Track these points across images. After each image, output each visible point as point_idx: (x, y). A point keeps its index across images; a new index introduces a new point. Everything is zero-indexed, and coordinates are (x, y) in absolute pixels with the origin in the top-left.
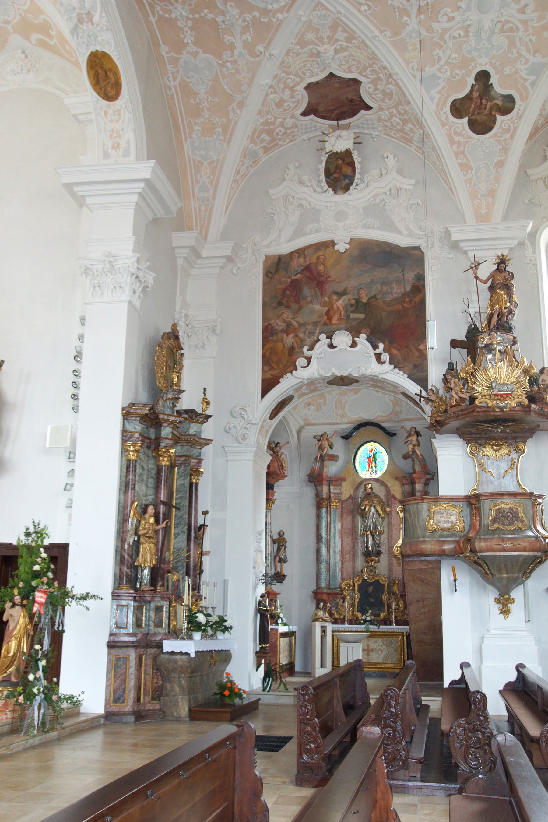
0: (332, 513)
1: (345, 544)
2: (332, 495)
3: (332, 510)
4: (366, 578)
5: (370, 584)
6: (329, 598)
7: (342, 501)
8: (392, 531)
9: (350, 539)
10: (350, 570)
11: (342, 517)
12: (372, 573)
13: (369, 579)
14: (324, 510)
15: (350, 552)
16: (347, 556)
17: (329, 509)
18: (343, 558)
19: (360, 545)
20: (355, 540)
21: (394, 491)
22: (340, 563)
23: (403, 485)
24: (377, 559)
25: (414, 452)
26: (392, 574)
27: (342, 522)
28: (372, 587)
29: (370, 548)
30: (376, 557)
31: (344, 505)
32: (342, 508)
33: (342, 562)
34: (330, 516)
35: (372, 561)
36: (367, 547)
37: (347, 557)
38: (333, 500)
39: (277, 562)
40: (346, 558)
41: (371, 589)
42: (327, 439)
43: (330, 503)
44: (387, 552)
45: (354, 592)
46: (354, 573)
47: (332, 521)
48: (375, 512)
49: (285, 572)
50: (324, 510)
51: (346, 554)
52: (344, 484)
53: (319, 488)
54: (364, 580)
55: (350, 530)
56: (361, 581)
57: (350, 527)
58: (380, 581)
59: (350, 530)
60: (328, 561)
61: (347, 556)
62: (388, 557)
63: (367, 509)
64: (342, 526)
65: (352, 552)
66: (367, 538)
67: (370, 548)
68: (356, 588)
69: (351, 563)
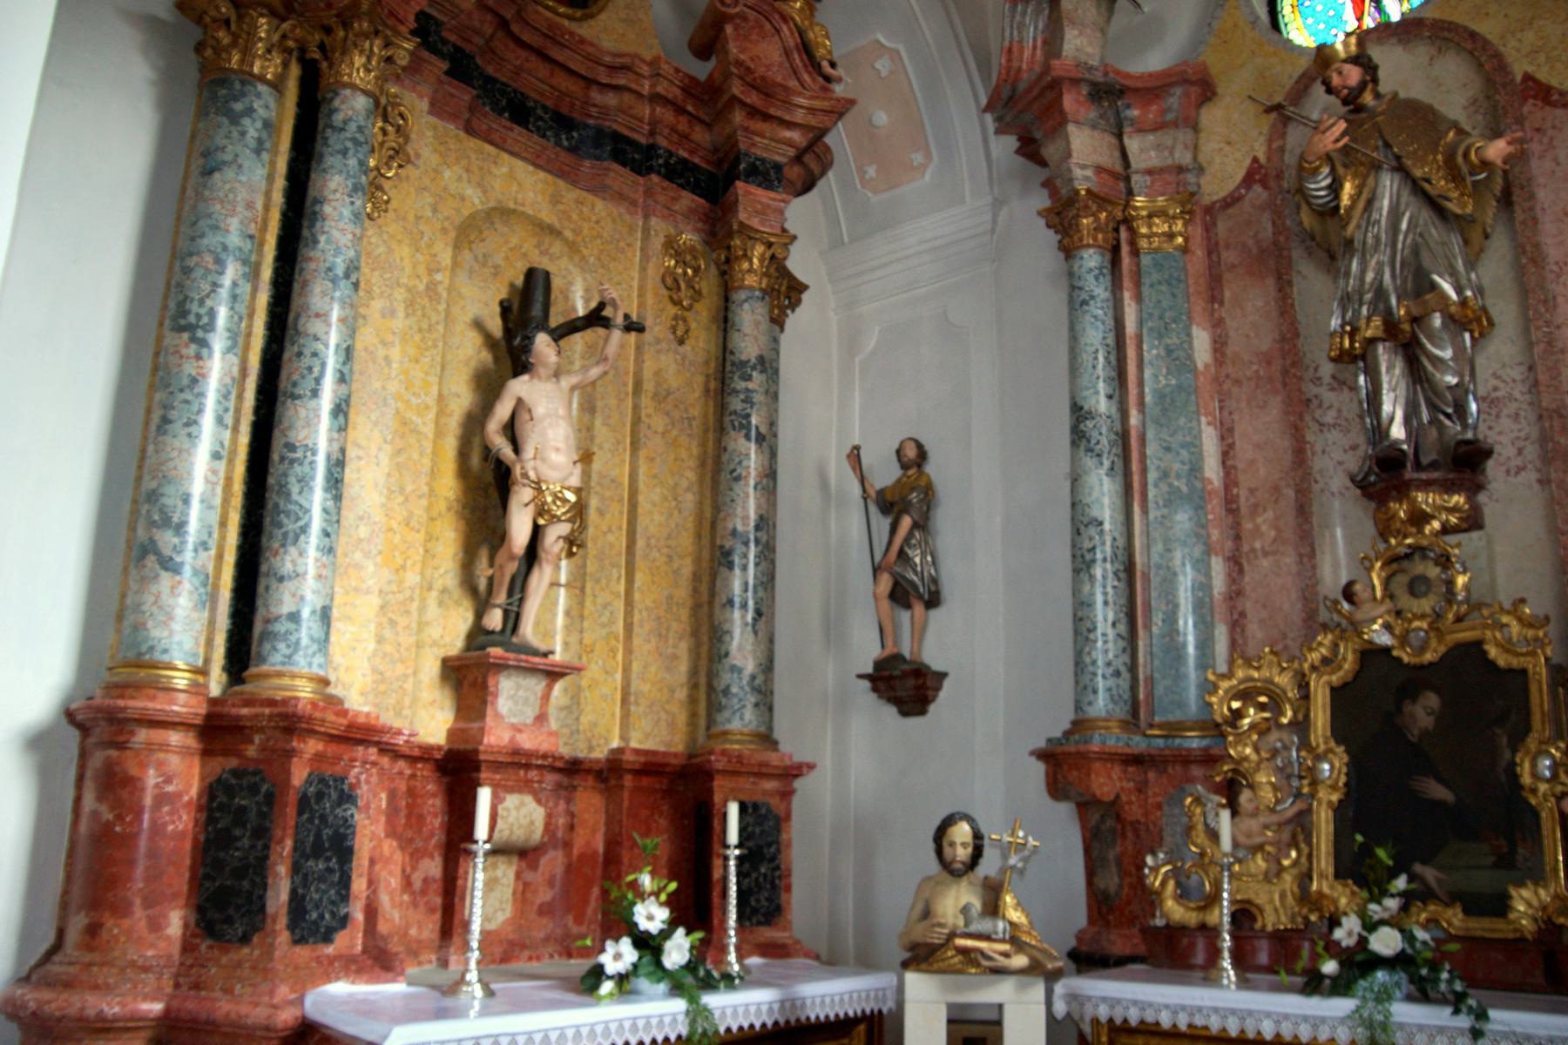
1: (1244, 451)
3: (1145, 260)
5: (1415, 680)
6: (1141, 789)
7: (1209, 210)
10: (1290, 606)
12: (1426, 605)
13: (1403, 640)
15: (1276, 489)
16: (1264, 521)
17: (1126, 260)
18: (1238, 538)
20: (1299, 409)
27: (1217, 324)
28: (1432, 700)
29: (1398, 432)
30: (1449, 488)
31: (1222, 227)
32: (1212, 249)
37: (1264, 526)
40: (1257, 531)
44: (1531, 451)
46: (1310, 616)
48: (1406, 196)
49: (933, 657)
51: (1255, 510)
52: (1211, 116)
54: (1372, 655)
55: (1267, 360)
56: (1349, 663)
57: (1266, 343)
58: (1493, 652)
59: (1267, 360)
61: (1264, 521)
62: (1544, 482)
64: (1219, 346)
65: (1290, 493)
67: (1398, 432)
68: (1321, 717)
69: (1289, 560)
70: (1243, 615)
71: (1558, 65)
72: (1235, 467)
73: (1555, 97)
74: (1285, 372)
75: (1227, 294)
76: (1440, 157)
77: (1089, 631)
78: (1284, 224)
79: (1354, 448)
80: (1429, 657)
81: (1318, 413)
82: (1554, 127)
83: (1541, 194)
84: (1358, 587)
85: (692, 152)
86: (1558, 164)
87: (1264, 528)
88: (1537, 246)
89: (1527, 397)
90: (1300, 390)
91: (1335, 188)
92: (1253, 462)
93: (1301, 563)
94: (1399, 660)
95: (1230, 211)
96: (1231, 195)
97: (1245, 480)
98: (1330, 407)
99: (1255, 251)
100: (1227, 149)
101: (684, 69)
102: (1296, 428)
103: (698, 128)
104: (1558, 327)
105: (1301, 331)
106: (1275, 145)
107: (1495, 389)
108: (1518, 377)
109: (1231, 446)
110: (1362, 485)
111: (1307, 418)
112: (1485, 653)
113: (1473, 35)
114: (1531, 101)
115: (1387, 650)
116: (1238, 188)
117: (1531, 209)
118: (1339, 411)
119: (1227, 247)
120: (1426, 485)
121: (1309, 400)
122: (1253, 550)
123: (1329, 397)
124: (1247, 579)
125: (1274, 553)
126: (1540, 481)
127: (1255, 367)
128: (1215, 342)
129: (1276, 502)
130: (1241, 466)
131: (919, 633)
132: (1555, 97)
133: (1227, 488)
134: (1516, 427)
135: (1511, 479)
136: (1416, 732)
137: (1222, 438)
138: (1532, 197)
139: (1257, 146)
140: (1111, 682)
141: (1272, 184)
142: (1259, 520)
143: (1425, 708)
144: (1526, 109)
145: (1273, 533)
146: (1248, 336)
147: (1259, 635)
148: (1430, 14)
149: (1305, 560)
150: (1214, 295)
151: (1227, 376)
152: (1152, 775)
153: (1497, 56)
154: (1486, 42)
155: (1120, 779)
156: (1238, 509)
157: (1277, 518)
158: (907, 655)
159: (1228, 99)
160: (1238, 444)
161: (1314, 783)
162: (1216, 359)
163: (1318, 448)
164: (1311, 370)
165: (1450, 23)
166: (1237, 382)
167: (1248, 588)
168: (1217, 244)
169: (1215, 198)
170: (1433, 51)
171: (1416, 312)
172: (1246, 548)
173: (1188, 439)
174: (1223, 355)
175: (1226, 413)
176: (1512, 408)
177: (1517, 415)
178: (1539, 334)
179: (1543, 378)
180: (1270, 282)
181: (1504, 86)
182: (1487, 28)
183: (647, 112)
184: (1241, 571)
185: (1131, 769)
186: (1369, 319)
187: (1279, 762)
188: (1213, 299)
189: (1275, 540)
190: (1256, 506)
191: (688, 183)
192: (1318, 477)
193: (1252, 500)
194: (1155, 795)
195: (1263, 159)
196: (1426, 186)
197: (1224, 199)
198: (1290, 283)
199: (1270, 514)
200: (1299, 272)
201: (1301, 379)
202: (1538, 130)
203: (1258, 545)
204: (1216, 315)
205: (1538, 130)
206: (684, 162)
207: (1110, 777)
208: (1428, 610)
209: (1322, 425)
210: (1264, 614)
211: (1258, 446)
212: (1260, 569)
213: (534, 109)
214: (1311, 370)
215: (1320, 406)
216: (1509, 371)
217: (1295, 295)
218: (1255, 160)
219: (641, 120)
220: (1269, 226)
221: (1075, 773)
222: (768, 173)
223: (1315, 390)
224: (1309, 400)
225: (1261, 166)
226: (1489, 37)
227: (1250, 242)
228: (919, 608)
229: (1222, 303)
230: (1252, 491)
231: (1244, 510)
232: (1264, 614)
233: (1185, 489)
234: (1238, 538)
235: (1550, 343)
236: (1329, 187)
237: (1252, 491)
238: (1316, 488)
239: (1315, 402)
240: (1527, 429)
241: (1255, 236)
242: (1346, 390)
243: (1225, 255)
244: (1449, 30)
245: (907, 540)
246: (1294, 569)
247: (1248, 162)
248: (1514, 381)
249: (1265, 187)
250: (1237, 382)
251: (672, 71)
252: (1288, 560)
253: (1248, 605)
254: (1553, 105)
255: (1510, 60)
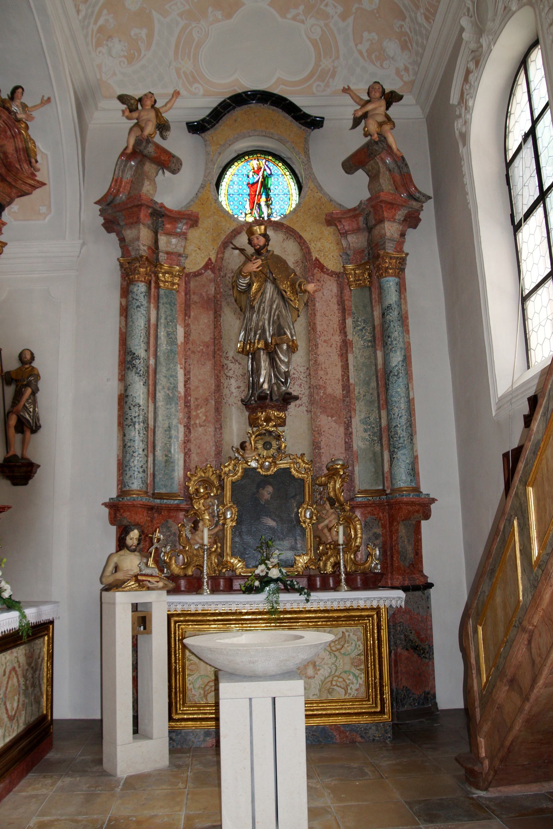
0: (163, 300)
1: (194, 382)
2: (162, 257)
3: (162, 292)
4: (254, 464)
7: (187, 275)
8: (316, 346)
9: (209, 366)
11: (187, 314)
13: (262, 466)
14: (140, 288)
15: (207, 400)
18: (189, 418)
19: (233, 383)
21: (320, 251)
22: (181, 429)
23: (344, 234)
24: (282, 414)
25: (383, 138)
26: (320, 455)
27: (187, 326)
28: (270, 489)
31: (192, 284)
33: (188, 428)
34: (158, 308)
35: (268, 420)
36: (254, 385)
38: (166, 267)
39: (12, 431)
40: (197, 416)
41: (267, 492)
42: (153, 106)
43: (156, 274)
45: (222, 503)
46: (218, 453)
47: (162, 321)
48: (275, 295)
50: (140, 288)
51: (197, 407)
52: (193, 234)
53: (129, 234)
54: (249, 472)
60: (151, 422)
63: (255, 286)
64: (187, 335)
66: (255, 359)
67: (266, 386)
69: (211, 429)
70: (189, 450)
71: (327, 258)
72: (190, 388)
73: (325, 270)
74: (215, 352)
75: (192, 314)
76: (289, 283)
77: (134, 452)
78: (220, 290)
79: (239, 387)
80: (269, 473)
81: (226, 371)
82: (323, 281)
83: (317, 304)
84: (247, 444)
86: (324, 295)
87: (200, 415)
88: (314, 324)
89: (305, 379)
90: (220, 361)
91: (250, 285)
92: (198, 387)
93: (215, 431)
94: (259, 472)
95: (197, 278)
96: (198, 271)
97: (194, 394)
98: (231, 369)
99: (206, 298)
100: (198, 251)
102: (217, 375)
104: (318, 355)
105: (223, 336)
106: (219, 256)
107: (294, 374)
108: (303, 371)
109: (189, 379)
110: (246, 403)
111: (222, 373)
112: (291, 472)
113: (301, 237)
114: (317, 269)
115: (255, 469)
116: (201, 269)
117: (314, 309)
118: (234, 372)
119: (194, 293)
120: (272, 408)
121: (223, 366)
122: (195, 424)
123: (231, 366)
124: (192, 436)
125: (204, 426)
126: (307, 411)
127: (201, 347)
128: (185, 333)
129: (206, 405)
130: (192, 388)
131: (24, 443)
132: (325, 270)
133: (186, 396)
134: (300, 389)
135: (296, 408)
136: (263, 500)
137: (185, 375)
138: (314, 305)
139: (211, 254)
140: (141, 475)
141: (216, 272)
142: (199, 412)
143: (267, 492)
144: (315, 271)
145: (204, 418)
146: (199, 334)
147: (196, 459)
148: (285, 222)
149: (217, 430)
150: (187, 314)
151: (189, 349)
152: (156, 515)
153: (308, 248)
154: (305, 241)
155: (146, 516)
156: (190, 406)
157: (206, 412)
158: (19, 454)
159: (201, 230)
160: (192, 379)
161: (225, 519)
162: (185, 341)
163: (225, 386)
164: (225, 354)
165: (293, 229)
166: (193, 352)
167: (192, 439)
168: (189, 291)
169: (191, 271)
170: (285, 237)
171: (278, 342)
172: (192, 422)
173: (173, 373)
174: (188, 339)
175: (187, 365)
176: (299, 382)
177: (301, 385)
178: (313, 357)
179: (312, 373)
180: (211, 313)
181: (309, 260)
182: (306, 236)
184: (190, 432)
185: (150, 512)
186: (259, 340)
187: (210, 511)
188: (186, 315)
189: (204, 421)
190: (198, 405)
192: (225, 397)
193: (196, 403)
194: (157, 523)
195: (213, 260)
196: (284, 293)
197: (195, 272)
198: (220, 316)
199: (203, 410)
200: (224, 312)
201: (221, 356)
202: (318, 280)
203: (197, 422)
204: (186, 322)
205: (318, 280)
207: (143, 515)
208: (270, 455)
209: (227, 376)
210: (199, 451)
211: (200, 381)
212: (198, 432)
214: (225, 354)
215: (227, 368)
216: (299, 368)
217: (221, 321)
218: (210, 259)
220: (213, 289)
221: (128, 513)
223: (226, 362)
224: (223, 366)
225: (212, 263)
226: (306, 240)
227: (204, 294)
228: (28, 433)
229: (189, 317)
230: (197, 399)
231: (192, 407)
232: (199, 451)
233: (171, 395)
234: (189, 418)
235: (316, 361)
236: (247, 283)
237: (197, 399)
238: (224, 401)
239: (225, 367)
240: (304, 391)
241: (207, 291)
242: (237, 364)
243: (192, 297)
244: (293, 232)
245: (27, 400)
246: (212, 433)
247: (207, 259)
248: (301, 372)
249: (213, 272)
250: (193, 352)
252: (210, 429)
253: (192, 447)
254: (324, 272)
255: (312, 251)
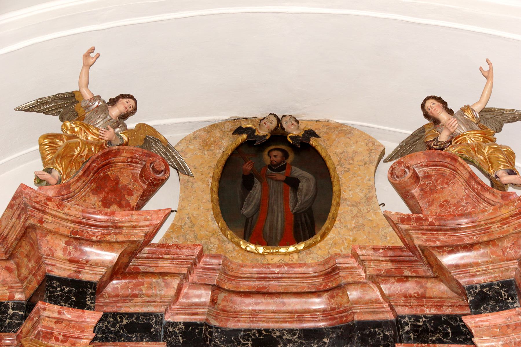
85: (439, 306)
101: (381, 244)
103: (429, 284)
183: (378, 293)
191: (446, 335)
206: (436, 318)
213: (281, 337)
219: (377, 301)
222: (499, 294)
251: (371, 252)
